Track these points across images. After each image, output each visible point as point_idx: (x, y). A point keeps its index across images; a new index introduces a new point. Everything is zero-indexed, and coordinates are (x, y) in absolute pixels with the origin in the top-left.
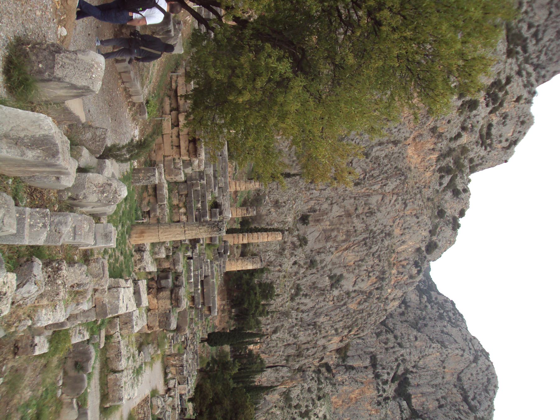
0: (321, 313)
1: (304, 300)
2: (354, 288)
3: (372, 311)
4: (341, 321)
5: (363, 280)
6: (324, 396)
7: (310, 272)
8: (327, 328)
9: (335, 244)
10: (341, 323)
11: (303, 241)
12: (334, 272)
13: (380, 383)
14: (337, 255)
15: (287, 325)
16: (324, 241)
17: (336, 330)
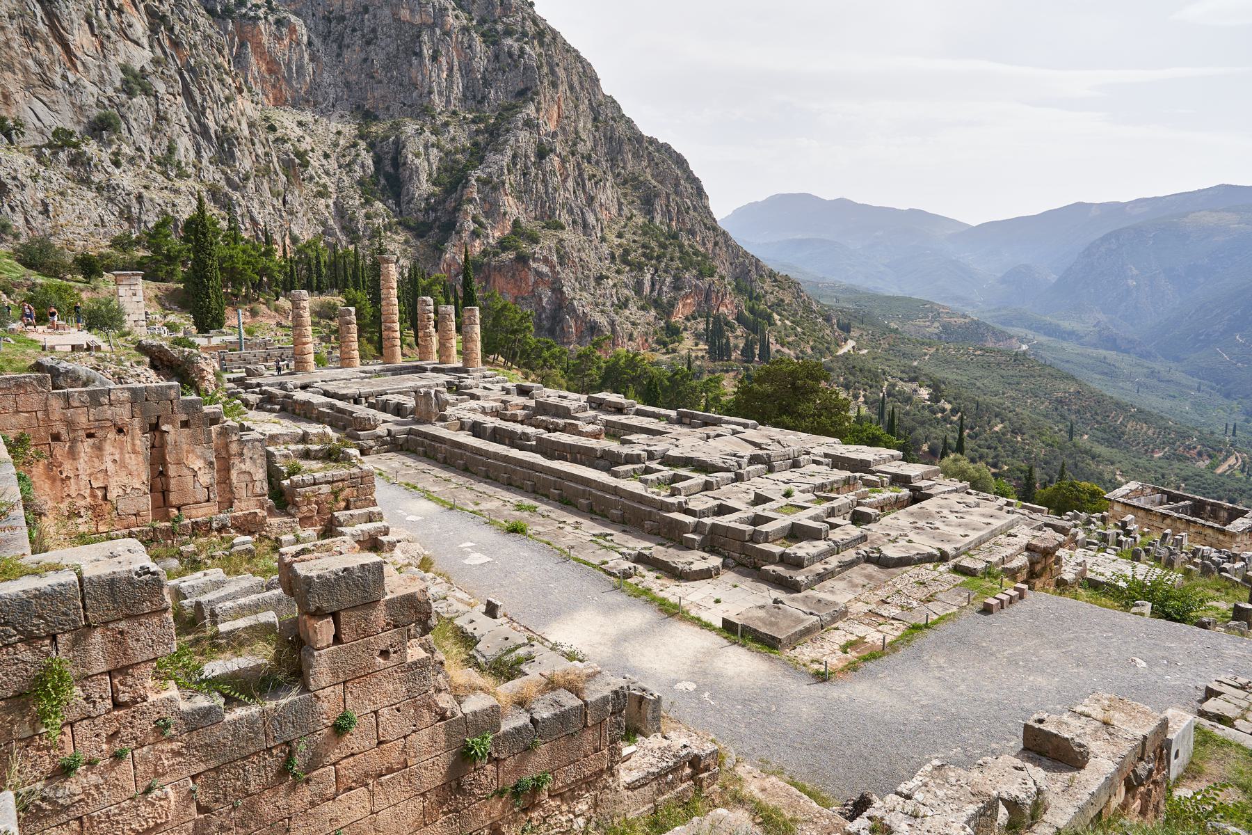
0: (198, 122)
1: (180, 155)
2: (146, 46)
3: (187, 22)
4: (212, 87)
5: (130, 26)
6: (267, 119)
7: (125, 133)
8: (226, 116)
9: (57, 69)
10: (215, 87)
11: (62, 139)
12: (118, 84)
13: (244, 11)
14: (80, 68)
15: (236, 196)
16: (53, 91)
17: (228, 99)
